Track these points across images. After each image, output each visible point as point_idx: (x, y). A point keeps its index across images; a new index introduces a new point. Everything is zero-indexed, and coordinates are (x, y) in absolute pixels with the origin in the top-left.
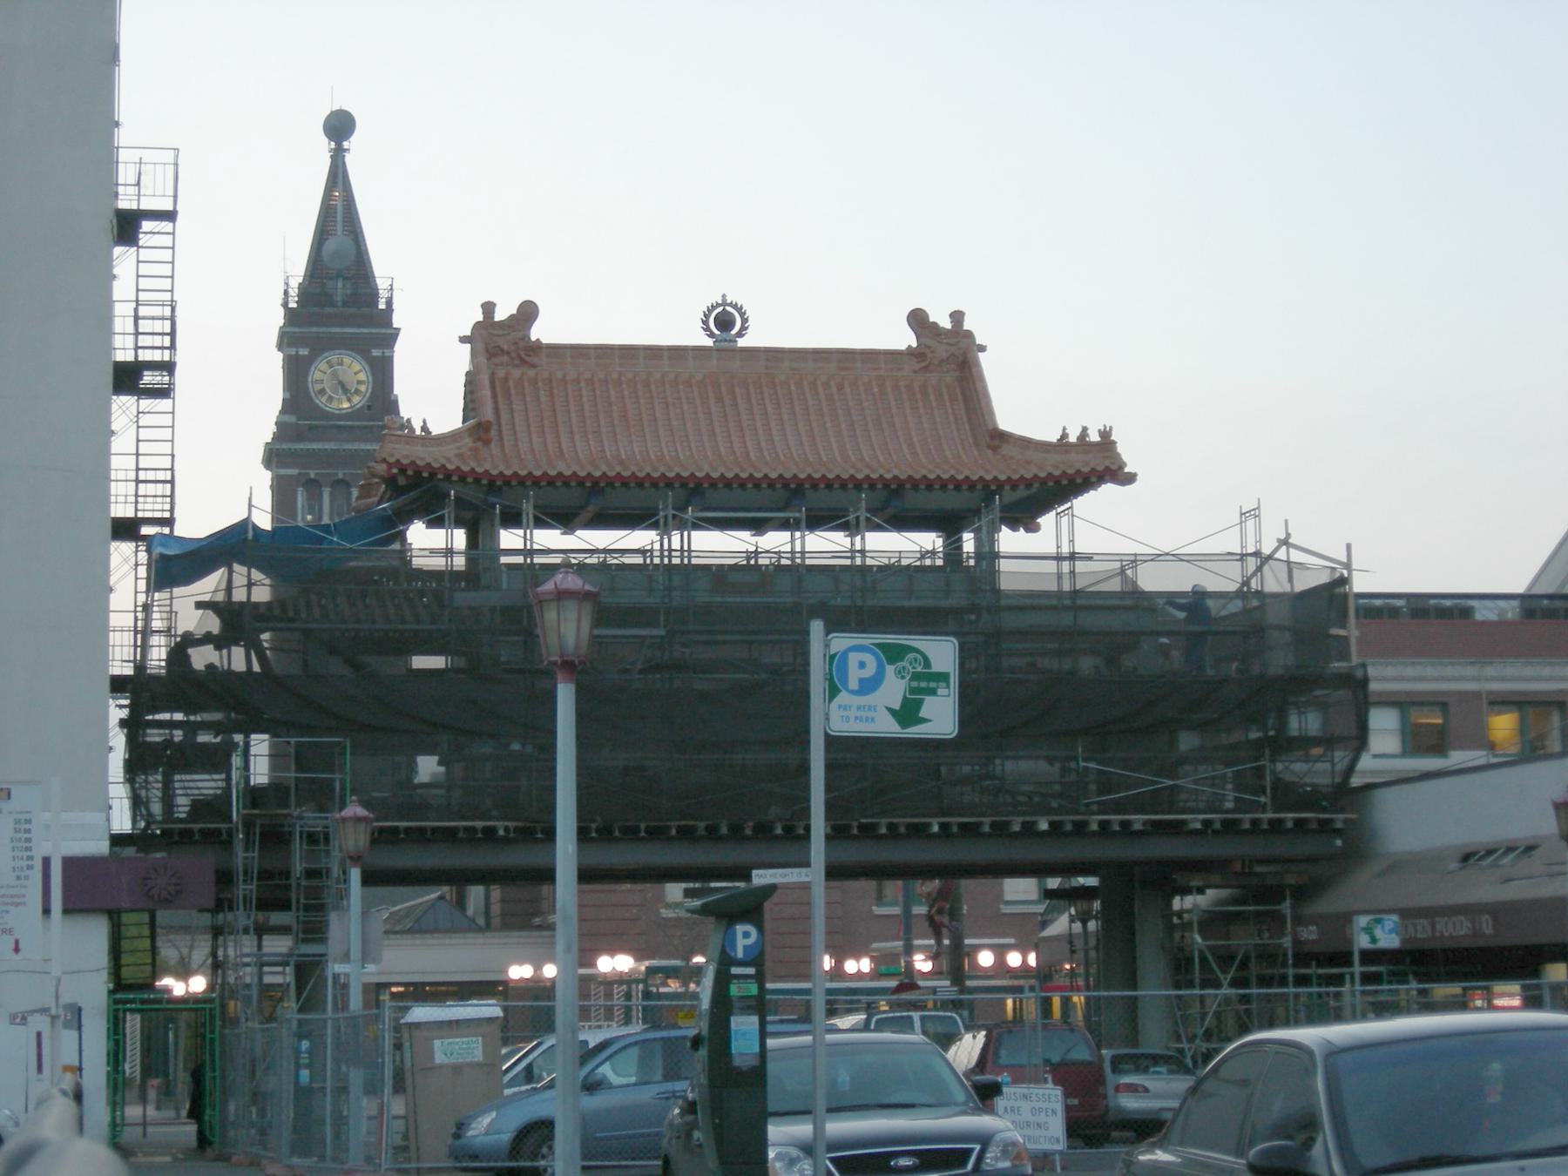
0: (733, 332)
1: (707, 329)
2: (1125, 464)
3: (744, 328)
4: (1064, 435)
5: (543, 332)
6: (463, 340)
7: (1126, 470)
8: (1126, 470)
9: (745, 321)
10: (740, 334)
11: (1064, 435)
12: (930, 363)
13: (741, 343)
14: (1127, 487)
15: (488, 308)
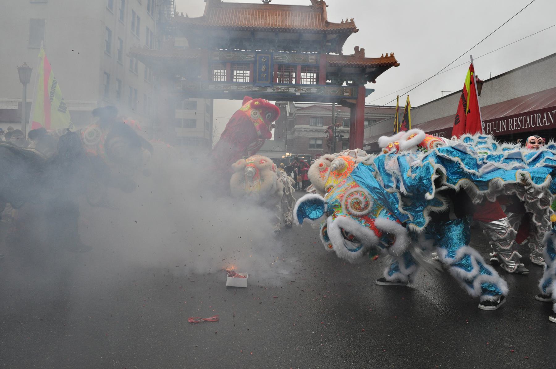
2: (397, 62)
4: (343, 21)
7: (397, 63)
8: (356, 28)
11: (343, 21)
13: (270, 3)
14: (356, 33)
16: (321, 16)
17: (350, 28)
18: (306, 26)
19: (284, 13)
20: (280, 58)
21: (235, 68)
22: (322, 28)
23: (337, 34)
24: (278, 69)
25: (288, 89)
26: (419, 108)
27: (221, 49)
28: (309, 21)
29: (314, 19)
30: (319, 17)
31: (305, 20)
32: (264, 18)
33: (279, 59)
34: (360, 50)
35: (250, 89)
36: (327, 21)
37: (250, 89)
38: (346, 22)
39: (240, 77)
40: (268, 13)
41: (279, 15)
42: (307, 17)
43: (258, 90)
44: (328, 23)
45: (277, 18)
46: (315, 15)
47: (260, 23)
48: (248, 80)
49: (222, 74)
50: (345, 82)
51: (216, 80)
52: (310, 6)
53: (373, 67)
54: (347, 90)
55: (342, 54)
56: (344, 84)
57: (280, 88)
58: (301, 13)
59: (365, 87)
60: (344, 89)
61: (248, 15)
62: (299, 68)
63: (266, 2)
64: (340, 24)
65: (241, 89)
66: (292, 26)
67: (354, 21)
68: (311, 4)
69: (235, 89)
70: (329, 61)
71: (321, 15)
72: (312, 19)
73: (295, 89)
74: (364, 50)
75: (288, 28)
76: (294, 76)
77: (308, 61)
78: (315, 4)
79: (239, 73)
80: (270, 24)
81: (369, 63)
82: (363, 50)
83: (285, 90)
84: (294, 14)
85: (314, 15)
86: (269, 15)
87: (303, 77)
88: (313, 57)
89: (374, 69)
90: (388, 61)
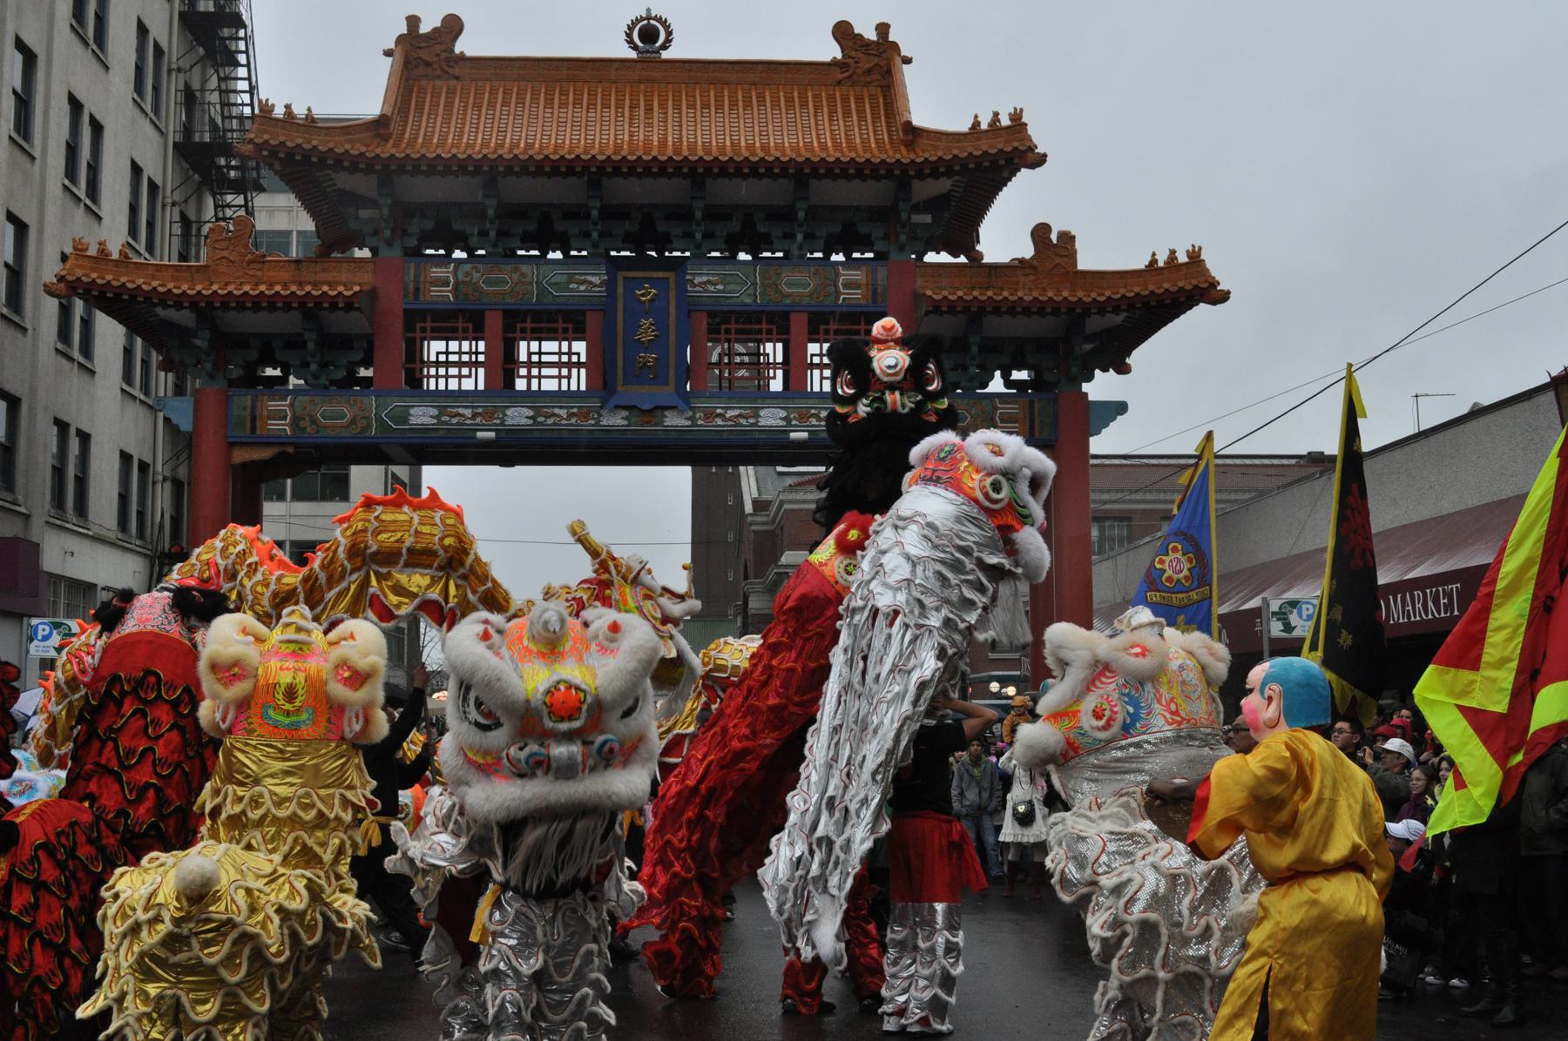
0: (658, 44)
1: (630, 41)
3: (668, 41)
4: (976, 124)
5: (466, 45)
6: (388, 53)
9: (669, 33)
10: (664, 47)
11: (976, 124)
12: (854, 73)
13: (665, 55)
15: (413, 21)
16: (882, 106)
17: (1009, 149)
18: (823, 147)
19: (726, 93)
20: (715, 284)
21: (523, 330)
22: (891, 153)
23: (957, 178)
24: (710, 331)
25: (757, 416)
26: (1325, 478)
27: (459, 254)
28: (831, 125)
29: (855, 117)
30: (874, 109)
31: (816, 120)
32: (642, 118)
33: (712, 289)
34: (1055, 241)
35: (593, 422)
36: (909, 123)
37: (593, 422)
38: (990, 125)
39: (545, 372)
40: (656, 99)
41: (705, 105)
42: (825, 109)
43: (625, 423)
44: (914, 133)
45: (699, 119)
46: (860, 100)
47: (626, 138)
48: (579, 381)
49: (465, 358)
50: (998, 374)
51: (442, 387)
52: (834, 63)
53: (1116, 310)
54: (1012, 409)
55: (980, 256)
56: (996, 385)
57: (719, 411)
58: (796, 94)
59: (1086, 394)
60: (996, 408)
61: (570, 107)
62: (799, 323)
63: (648, 52)
64: (964, 135)
65: (550, 421)
66: (763, 148)
67: (1024, 120)
68: (839, 56)
69: (524, 421)
70: (929, 292)
71: (881, 100)
72: (847, 113)
73: (783, 414)
74: (1074, 237)
75: (747, 158)
76: (780, 359)
77: (838, 293)
78: (853, 54)
79: (540, 353)
80: (670, 143)
81: (1099, 295)
82: (1067, 239)
83: (743, 421)
84: (768, 98)
85: (852, 100)
86: (663, 106)
87: (816, 360)
88: (857, 275)
89: (1119, 319)
90: (1181, 284)
